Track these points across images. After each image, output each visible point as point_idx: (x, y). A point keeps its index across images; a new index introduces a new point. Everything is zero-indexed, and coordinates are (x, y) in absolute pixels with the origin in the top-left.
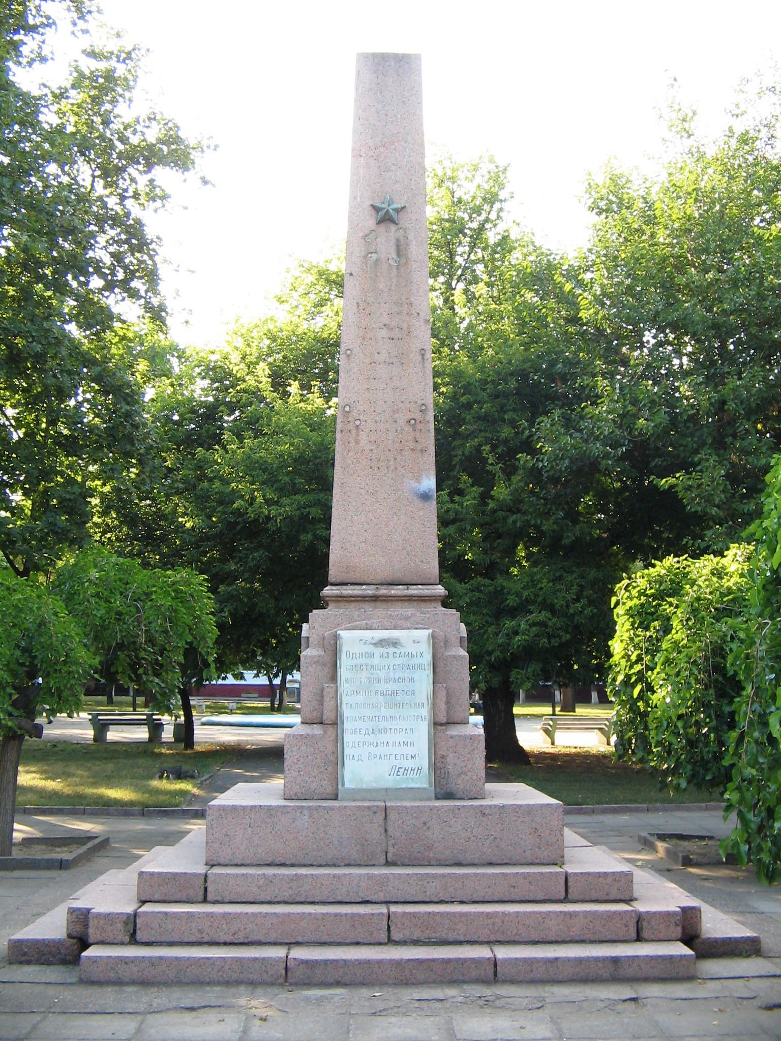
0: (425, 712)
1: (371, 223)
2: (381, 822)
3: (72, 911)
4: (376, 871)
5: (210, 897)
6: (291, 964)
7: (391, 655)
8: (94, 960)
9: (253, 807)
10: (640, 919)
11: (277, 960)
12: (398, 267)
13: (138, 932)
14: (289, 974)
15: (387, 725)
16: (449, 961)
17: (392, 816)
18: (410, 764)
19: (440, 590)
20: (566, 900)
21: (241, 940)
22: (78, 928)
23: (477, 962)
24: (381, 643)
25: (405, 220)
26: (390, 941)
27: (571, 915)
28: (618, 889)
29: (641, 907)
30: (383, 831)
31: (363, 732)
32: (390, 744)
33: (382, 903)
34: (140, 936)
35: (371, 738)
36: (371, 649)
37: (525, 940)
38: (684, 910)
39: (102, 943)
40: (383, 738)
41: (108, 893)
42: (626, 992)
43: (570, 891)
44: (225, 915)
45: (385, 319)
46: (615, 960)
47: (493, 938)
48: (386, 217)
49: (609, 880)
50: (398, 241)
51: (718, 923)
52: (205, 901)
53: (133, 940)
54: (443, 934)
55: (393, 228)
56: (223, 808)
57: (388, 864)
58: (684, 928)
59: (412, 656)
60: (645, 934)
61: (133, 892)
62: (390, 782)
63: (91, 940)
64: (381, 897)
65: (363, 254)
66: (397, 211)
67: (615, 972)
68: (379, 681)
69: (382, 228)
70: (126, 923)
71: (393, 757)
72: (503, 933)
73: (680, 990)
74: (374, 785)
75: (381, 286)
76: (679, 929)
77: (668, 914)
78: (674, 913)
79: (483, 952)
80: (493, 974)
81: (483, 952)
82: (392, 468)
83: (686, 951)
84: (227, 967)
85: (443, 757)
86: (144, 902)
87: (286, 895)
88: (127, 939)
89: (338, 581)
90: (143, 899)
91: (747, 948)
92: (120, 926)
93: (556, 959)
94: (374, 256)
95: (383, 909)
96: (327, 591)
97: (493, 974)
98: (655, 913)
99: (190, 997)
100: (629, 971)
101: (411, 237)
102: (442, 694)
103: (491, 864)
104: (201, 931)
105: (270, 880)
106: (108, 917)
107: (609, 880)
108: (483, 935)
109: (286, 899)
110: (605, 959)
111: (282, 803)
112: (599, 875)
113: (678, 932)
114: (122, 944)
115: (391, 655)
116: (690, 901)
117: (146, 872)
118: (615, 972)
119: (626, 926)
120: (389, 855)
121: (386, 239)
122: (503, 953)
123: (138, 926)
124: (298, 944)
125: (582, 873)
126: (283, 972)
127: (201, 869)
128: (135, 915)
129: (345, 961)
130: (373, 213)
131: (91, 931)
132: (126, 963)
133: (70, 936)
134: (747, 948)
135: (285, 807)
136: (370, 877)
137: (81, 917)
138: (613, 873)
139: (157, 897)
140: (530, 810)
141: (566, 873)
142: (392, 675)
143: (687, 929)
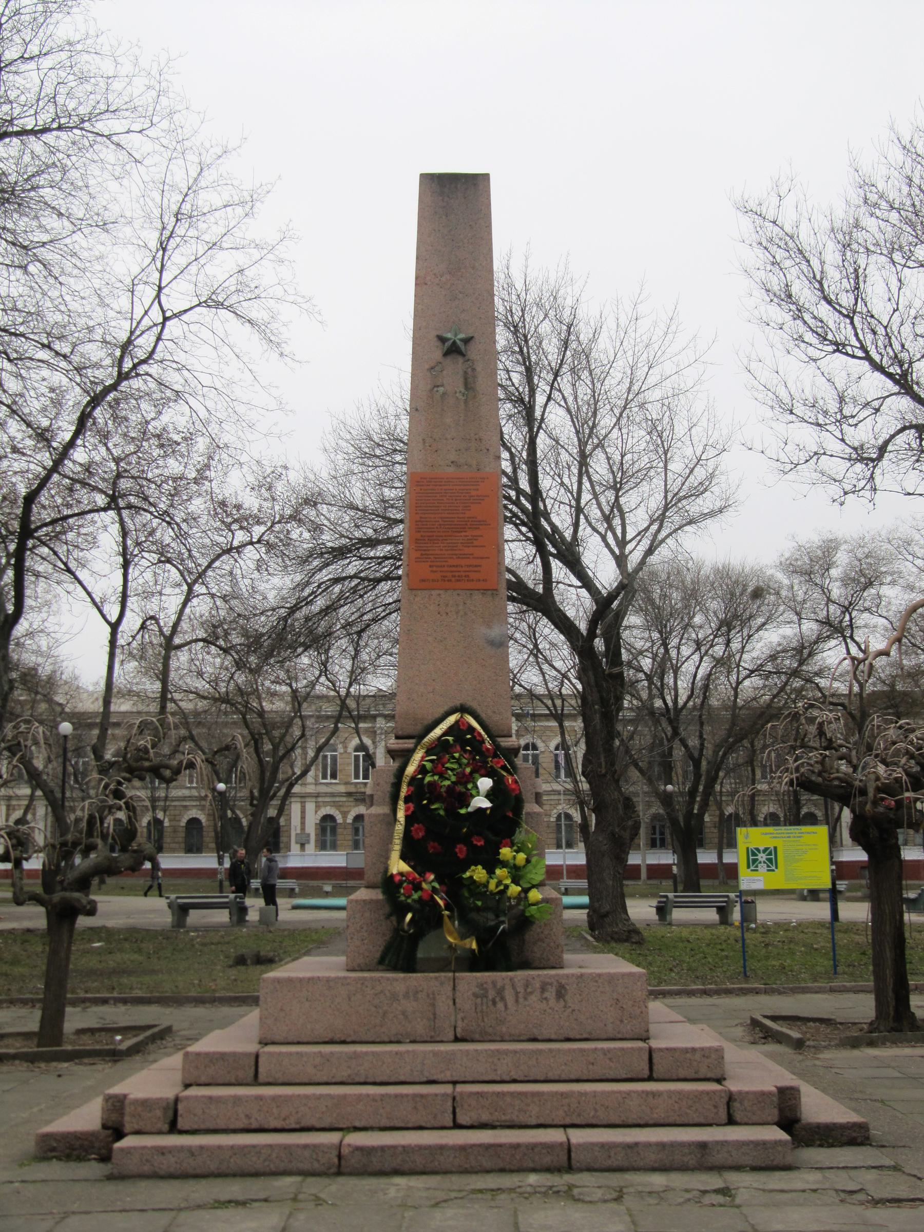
1: (438, 354)
2: (450, 994)
3: (108, 1098)
4: (442, 1047)
5: (262, 1077)
6: (345, 1151)
8: (128, 1151)
9: (310, 979)
10: (731, 1098)
11: (330, 1147)
12: (466, 402)
13: (180, 1119)
14: (343, 1162)
16: (517, 1146)
17: (461, 987)
20: (650, 1078)
21: (294, 1126)
22: (114, 1117)
23: (549, 1147)
25: (473, 352)
26: (457, 1126)
27: (655, 1094)
28: (707, 1067)
29: (733, 1086)
30: (451, 1003)
33: (448, 1082)
34: (181, 1124)
37: (605, 1122)
38: (782, 1091)
39: (138, 1132)
41: (150, 1081)
42: (714, 1181)
43: (655, 1068)
44: (274, 1098)
45: (453, 456)
46: (703, 1146)
47: (568, 1121)
48: (453, 350)
49: (697, 1056)
50: (466, 373)
51: (818, 1107)
52: (256, 1081)
53: (173, 1128)
54: (513, 1116)
55: (461, 360)
56: (278, 981)
57: (457, 1040)
58: (781, 1110)
60: (738, 1117)
61: (178, 1077)
63: (128, 1128)
64: (448, 1076)
65: (429, 387)
66: (467, 341)
67: (702, 1159)
69: (449, 361)
70: (166, 1109)
72: (579, 1115)
73: (776, 1180)
75: (448, 421)
76: (776, 1112)
77: (763, 1094)
78: (770, 1094)
79: (555, 1136)
80: (566, 1161)
81: (555, 1136)
82: (462, 613)
83: (783, 1136)
84: (274, 1155)
86: (187, 1086)
87: (343, 1075)
88: (166, 1127)
90: (188, 1082)
91: (853, 1136)
92: (159, 1113)
93: (637, 1144)
94: (441, 389)
95: (448, 1089)
97: (566, 1161)
98: (747, 1093)
99: (234, 1189)
100: (718, 1158)
101: (479, 369)
103: (568, 1040)
104: (248, 1117)
105: (327, 1058)
106: (145, 1103)
107: (697, 1056)
108: (559, 1117)
109: (344, 1079)
110: (690, 1144)
111: (343, 974)
112: (686, 1051)
113: (775, 1114)
114: (160, 1133)
116: (788, 1079)
117: (192, 1053)
118: (702, 1159)
119: (715, 1107)
120: (459, 1030)
121: (453, 371)
122: (578, 1136)
123: (180, 1112)
124: (357, 1129)
125: (667, 1049)
126: (336, 1160)
127: (253, 1048)
128: (177, 1100)
129: (403, 1147)
130: (439, 344)
131: (127, 1118)
132: (163, 1154)
133: (105, 1127)
134: (853, 1136)
135: (345, 978)
136: (436, 1054)
137: (117, 1104)
138: (702, 1049)
139: (203, 1079)
140: (612, 979)
141: (651, 1051)
143: (786, 1111)
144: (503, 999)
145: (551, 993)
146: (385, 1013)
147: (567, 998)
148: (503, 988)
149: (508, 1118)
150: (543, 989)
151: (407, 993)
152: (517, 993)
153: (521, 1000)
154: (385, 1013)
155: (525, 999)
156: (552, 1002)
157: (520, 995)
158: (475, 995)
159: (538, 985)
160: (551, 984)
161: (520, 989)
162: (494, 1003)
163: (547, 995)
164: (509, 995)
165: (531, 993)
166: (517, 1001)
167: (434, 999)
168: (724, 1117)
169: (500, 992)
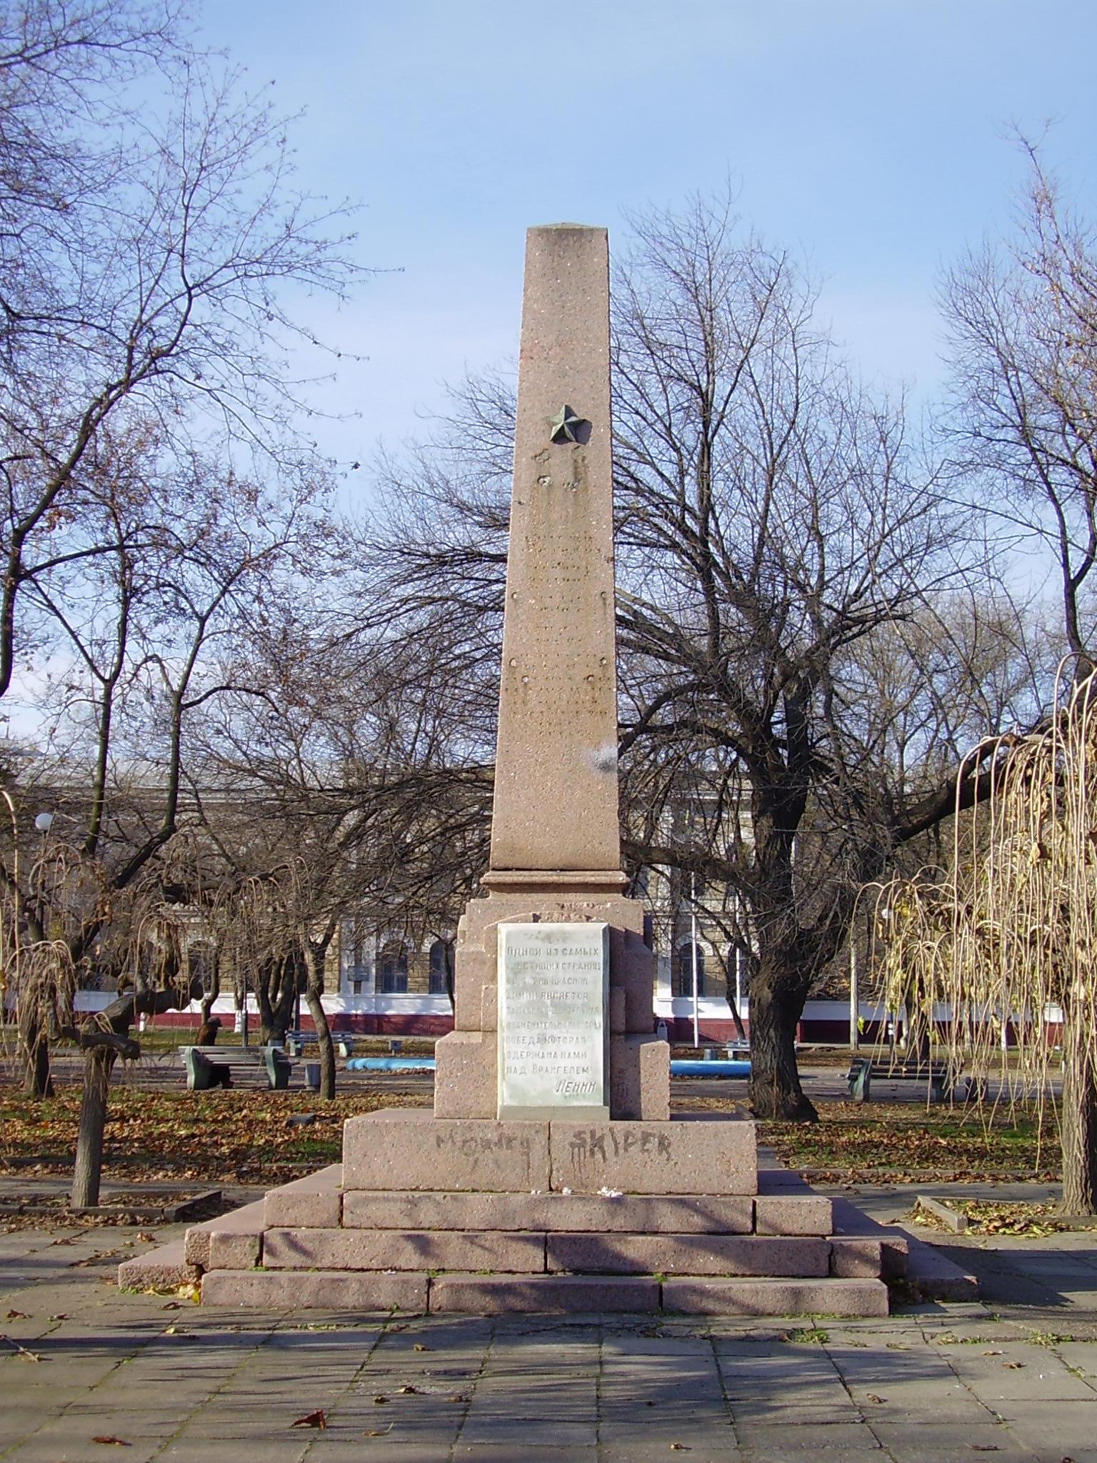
0: (599, 1019)
7: (560, 952)
15: (555, 1033)
18: (580, 1078)
19: (621, 877)
24: (549, 937)
31: (527, 1040)
32: (559, 1054)
35: (536, 1048)
36: (538, 944)
40: (551, 1047)
59: (586, 953)
62: (556, 1099)
68: (546, 983)
71: (561, 1070)
74: (539, 1103)
85: (621, 1071)
89: (502, 865)
96: (489, 877)
102: (621, 998)
115: (560, 952)
142: (561, 975)
144: (601, 1148)
145: (653, 1144)
146: (476, 1161)
147: (670, 1150)
148: (602, 1138)
149: (601, 1264)
150: (646, 1138)
151: (500, 1140)
152: (616, 1144)
153: (621, 1151)
154: (476, 1161)
155: (626, 1150)
156: (655, 1152)
157: (621, 1146)
158: (572, 1145)
159: (639, 1136)
160: (654, 1135)
161: (621, 1140)
162: (592, 1153)
163: (648, 1146)
164: (608, 1145)
165: (632, 1144)
166: (616, 1152)
167: (528, 1147)
168: (824, 1266)
169: (598, 1143)
